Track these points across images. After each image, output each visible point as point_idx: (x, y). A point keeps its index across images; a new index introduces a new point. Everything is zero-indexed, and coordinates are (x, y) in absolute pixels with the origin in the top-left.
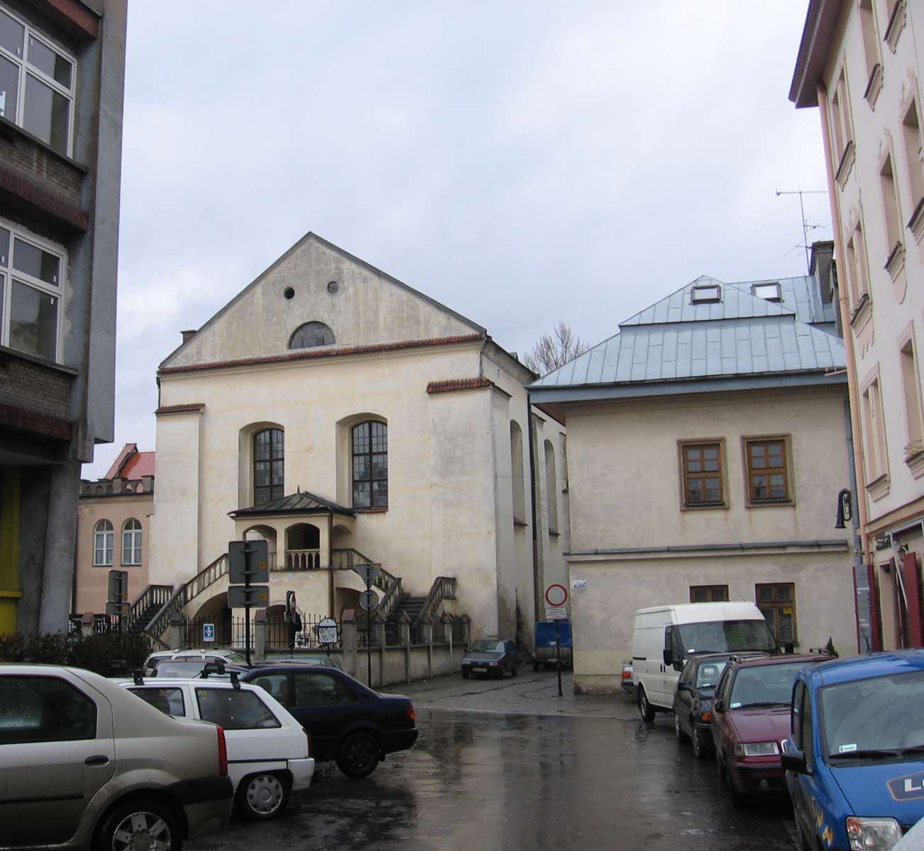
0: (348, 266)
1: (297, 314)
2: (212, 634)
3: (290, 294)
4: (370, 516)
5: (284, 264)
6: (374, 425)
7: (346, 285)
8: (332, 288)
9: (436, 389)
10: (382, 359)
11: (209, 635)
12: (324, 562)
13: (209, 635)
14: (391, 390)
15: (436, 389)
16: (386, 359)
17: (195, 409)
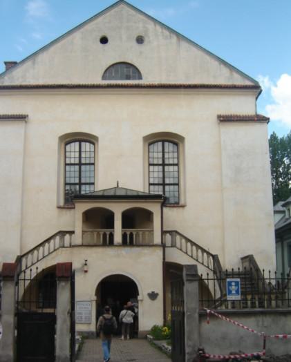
0: (151, 25)
1: (111, 55)
2: (237, 292)
3: (104, 40)
4: (172, 209)
5: (100, 19)
6: (166, 144)
7: (151, 38)
8: (140, 40)
9: (225, 119)
10: (180, 94)
11: (234, 292)
12: (157, 239)
13: (234, 292)
14: (192, 118)
15: (225, 119)
16: (184, 94)
17: (22, 118)
